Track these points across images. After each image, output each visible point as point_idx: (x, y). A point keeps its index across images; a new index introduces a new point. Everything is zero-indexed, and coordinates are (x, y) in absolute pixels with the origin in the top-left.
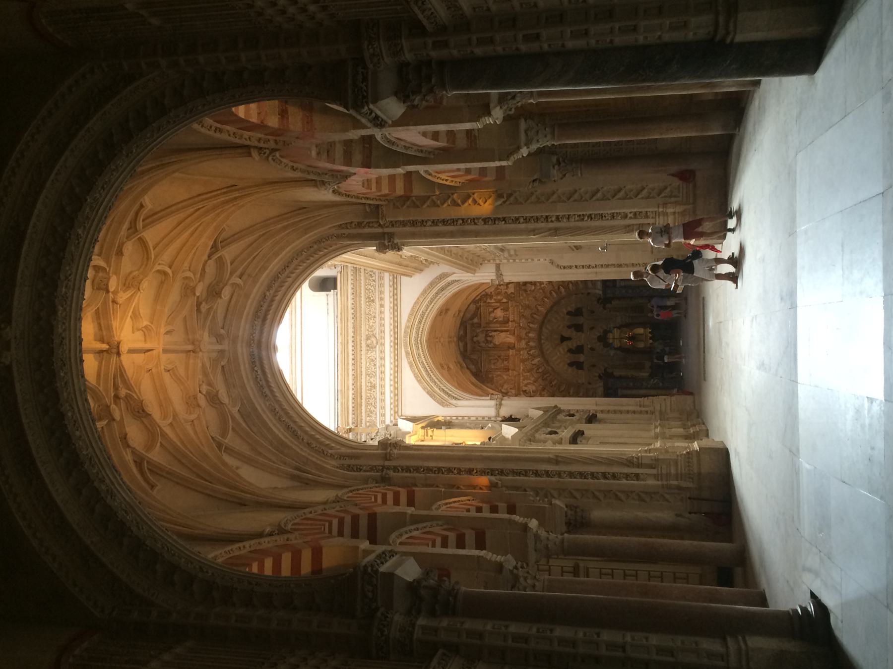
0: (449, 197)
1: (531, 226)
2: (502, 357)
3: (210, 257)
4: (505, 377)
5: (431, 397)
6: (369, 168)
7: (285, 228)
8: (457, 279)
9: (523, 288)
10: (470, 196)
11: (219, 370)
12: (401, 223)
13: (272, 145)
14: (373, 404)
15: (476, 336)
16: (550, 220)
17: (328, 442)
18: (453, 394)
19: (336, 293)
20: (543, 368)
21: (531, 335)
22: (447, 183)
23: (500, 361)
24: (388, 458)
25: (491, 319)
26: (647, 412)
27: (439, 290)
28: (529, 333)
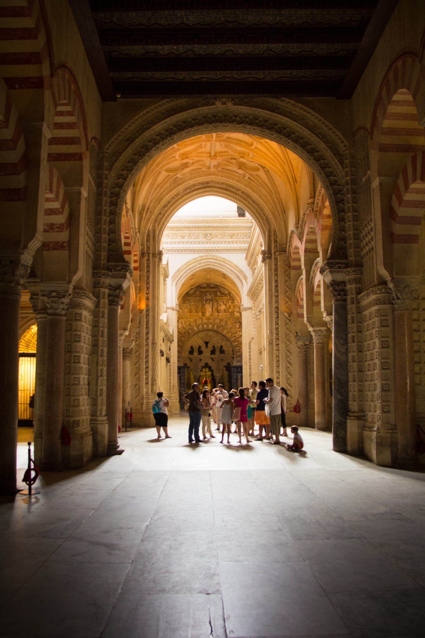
0: (290, 289)
1: (274, 331)
3: (259, 164)
4: (186, 311)
6: (305, 252)
7: (275, 203)
9: (237, 321)
10: (289, 299)
11: (200, 167)
13: (315, 209)
15: (210, 294)
17: (161, 223)
20: (191, 332)
21: (210, 326)
22: (297, 288)
23: (195, 308)
25: (219, 303)
26: (170, 389)
28: (212, 324)
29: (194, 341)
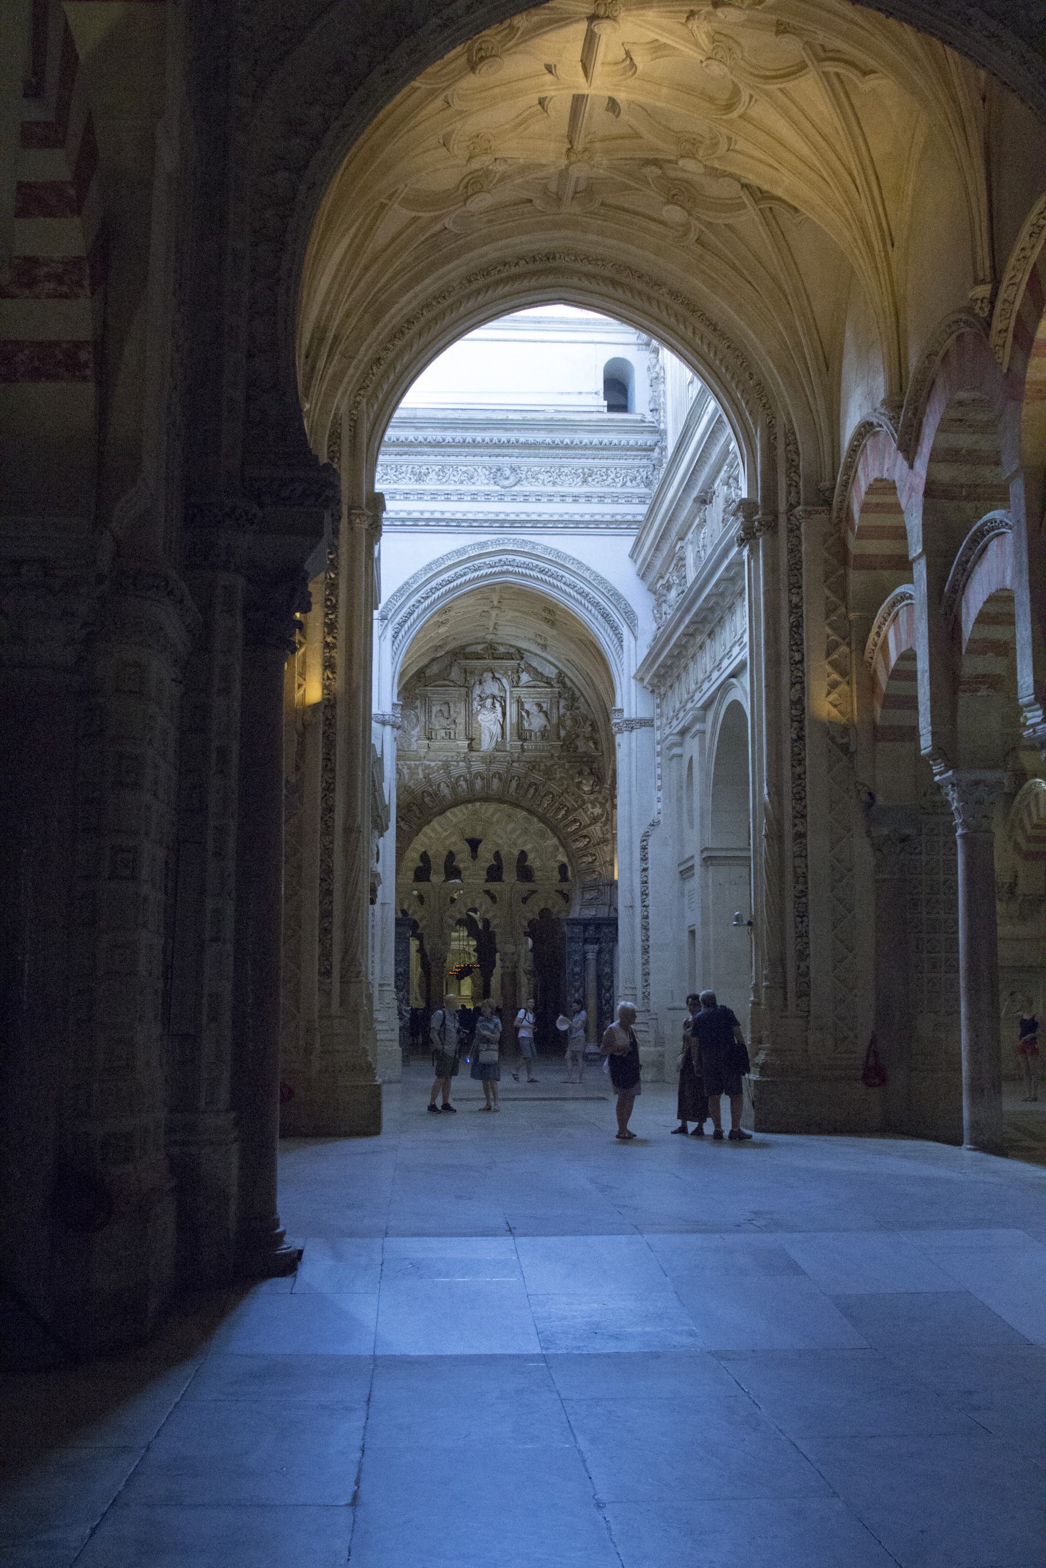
0: (844, 639)
1: (787, 788)
2: (454, 726)
5: (399, 591)
6: (927, 494)
8: (625, 643)
12: (797, 546)
14: (385, 477)
15: (494, 677)
16: (797, 821)
17: (380, 397)
18: (403, 632)
19: (601, 409)
20: (431, 804)
21: (496, 783)
22: (872, 635)
23: (445, 723)
24: (353, 511)
25: (526, 707)
27: (604, 608)
28: (500, 779)
29: (433, 835)
